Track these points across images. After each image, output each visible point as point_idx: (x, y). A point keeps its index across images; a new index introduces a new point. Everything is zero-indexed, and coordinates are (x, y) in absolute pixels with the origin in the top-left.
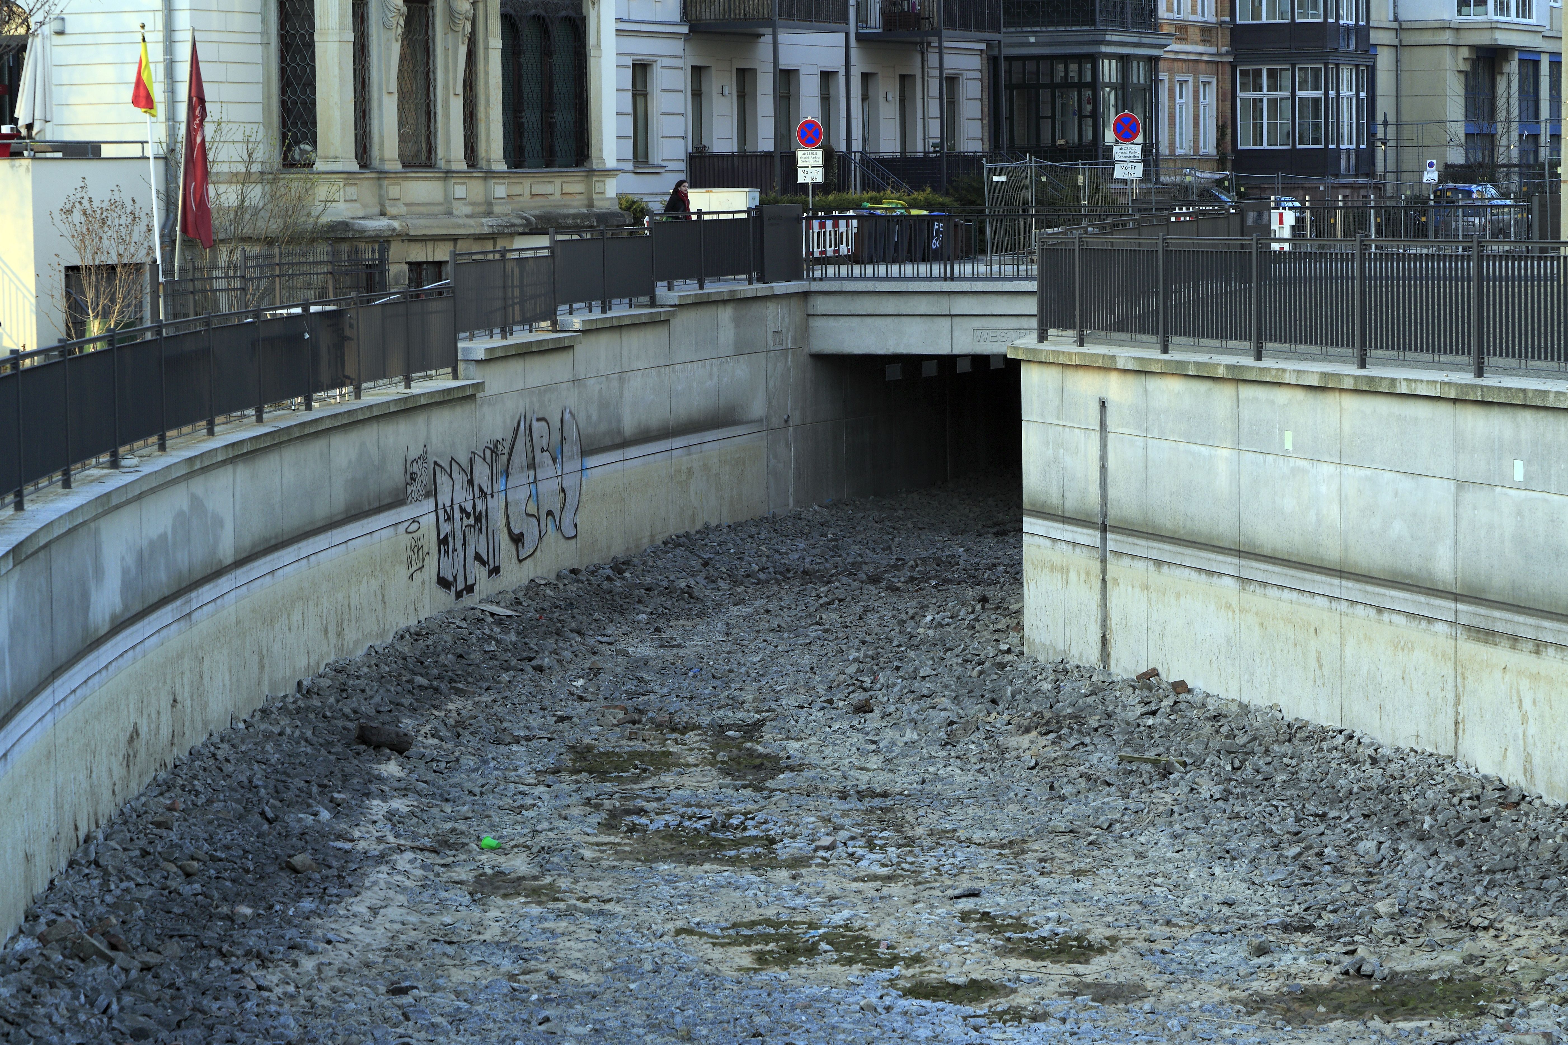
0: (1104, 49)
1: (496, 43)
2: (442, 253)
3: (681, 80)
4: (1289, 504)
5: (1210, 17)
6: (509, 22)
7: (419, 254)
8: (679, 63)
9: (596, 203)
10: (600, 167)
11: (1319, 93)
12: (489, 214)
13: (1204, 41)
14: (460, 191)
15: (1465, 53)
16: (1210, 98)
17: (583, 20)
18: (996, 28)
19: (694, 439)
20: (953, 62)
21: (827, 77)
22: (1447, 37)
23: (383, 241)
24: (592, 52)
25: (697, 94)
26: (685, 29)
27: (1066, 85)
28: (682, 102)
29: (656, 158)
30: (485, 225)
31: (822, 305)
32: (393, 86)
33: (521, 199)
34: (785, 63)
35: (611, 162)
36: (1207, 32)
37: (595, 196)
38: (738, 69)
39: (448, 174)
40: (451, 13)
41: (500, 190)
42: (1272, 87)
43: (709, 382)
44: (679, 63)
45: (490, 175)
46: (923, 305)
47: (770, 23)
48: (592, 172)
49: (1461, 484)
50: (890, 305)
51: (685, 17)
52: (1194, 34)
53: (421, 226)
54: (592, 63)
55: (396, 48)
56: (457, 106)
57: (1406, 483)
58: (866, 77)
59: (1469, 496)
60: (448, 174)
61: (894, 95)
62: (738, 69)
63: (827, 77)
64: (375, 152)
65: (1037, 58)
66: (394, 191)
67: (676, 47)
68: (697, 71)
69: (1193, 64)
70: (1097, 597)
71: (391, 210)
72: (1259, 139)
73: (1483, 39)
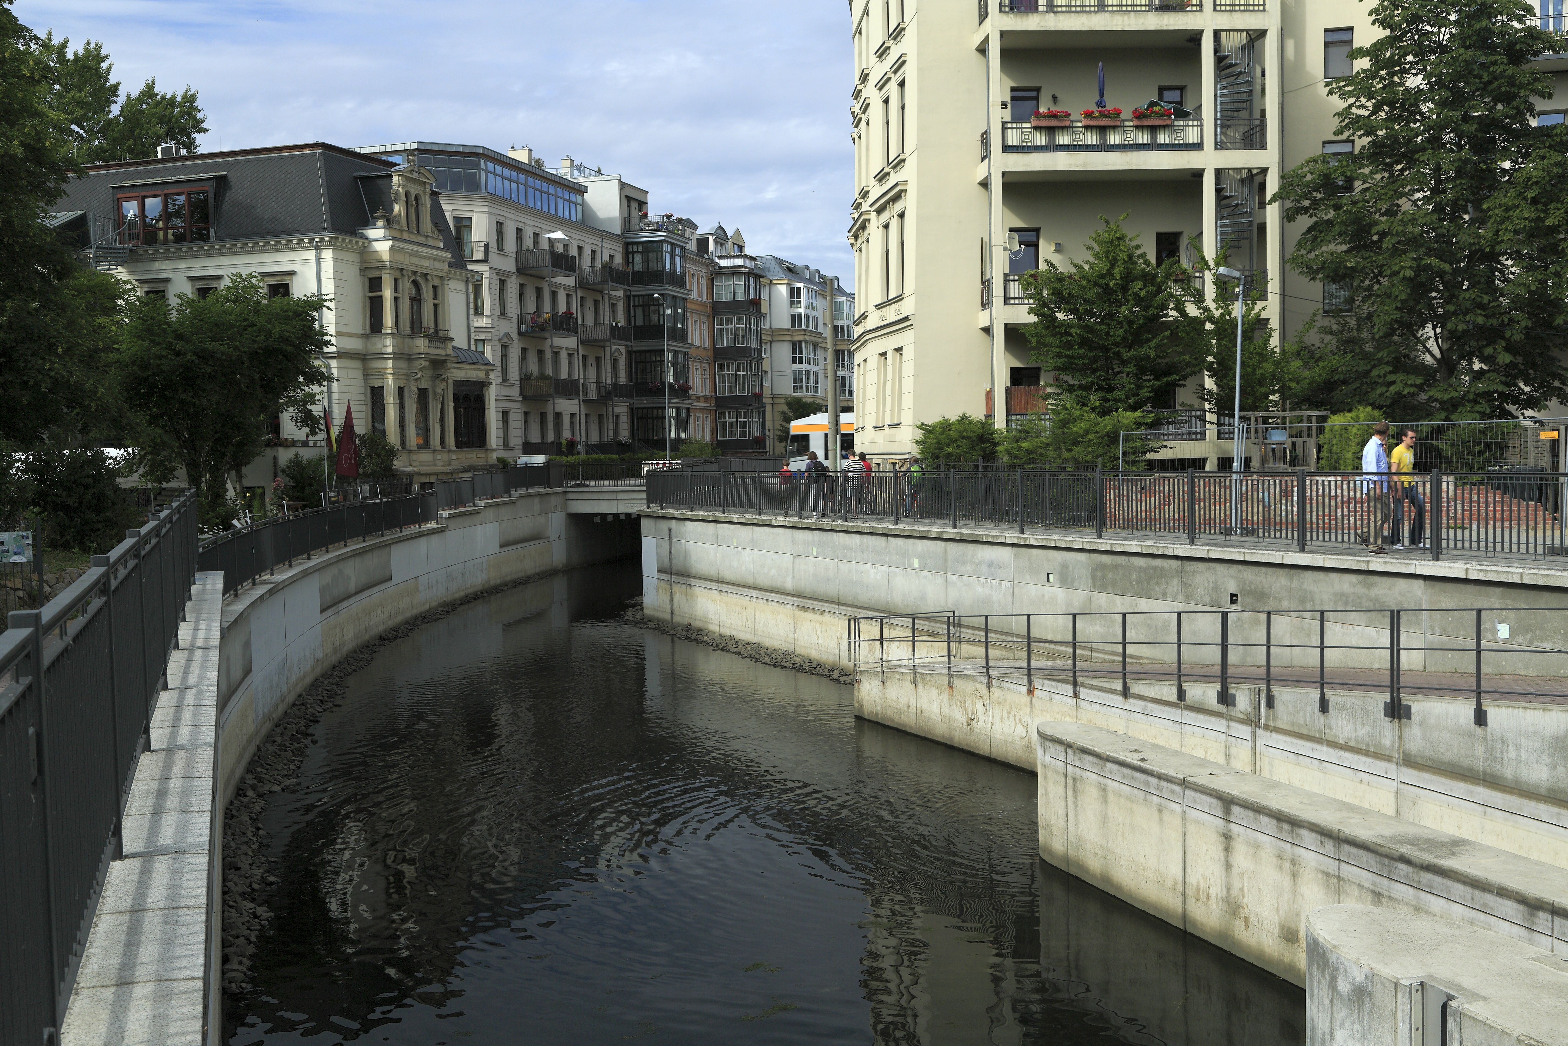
1: (451, 404)
2: (432, 479)
4: (735, 564)
5: (708, 394)
6: (456, 397)
7: (424, 480)
12: (450, 465)
14: (439, 457)
16: (708, 422)
17: (484, 395)
18: (632, 397)
19: (525, 544)
20: (617, 410)
21: (573, 415)
23: (411, 475)
24: (487, 407)
25: (526, 422)
29: (511, 444)
30: (448, 469)
31: (571, 496)
32: (414, 419)
34: (557, 410)
35: (494, 446)
36: (706, 399)
39: (435, 451)
40: (435, 394)
41: (454, 457)
45: (450, 451)
46: (607, 496)
47: (551, 396)
49: (795, 556)
50: (595, 496)
51: (521, 394)
52: (702, 399)
53: (425, 469)
54: (487, 411)
55: (415, 406)
56: (437, 427)
57: (775, 556)
58: (586, 415)
59: (798, 560)
60: (435, 451)
61: (597, 421)
63: (573, 415)
64: (407, 443)
66: (414, 457)
67: (518, 405)
69: (703, 410)
70: (669, 598)
71: (414, 464)
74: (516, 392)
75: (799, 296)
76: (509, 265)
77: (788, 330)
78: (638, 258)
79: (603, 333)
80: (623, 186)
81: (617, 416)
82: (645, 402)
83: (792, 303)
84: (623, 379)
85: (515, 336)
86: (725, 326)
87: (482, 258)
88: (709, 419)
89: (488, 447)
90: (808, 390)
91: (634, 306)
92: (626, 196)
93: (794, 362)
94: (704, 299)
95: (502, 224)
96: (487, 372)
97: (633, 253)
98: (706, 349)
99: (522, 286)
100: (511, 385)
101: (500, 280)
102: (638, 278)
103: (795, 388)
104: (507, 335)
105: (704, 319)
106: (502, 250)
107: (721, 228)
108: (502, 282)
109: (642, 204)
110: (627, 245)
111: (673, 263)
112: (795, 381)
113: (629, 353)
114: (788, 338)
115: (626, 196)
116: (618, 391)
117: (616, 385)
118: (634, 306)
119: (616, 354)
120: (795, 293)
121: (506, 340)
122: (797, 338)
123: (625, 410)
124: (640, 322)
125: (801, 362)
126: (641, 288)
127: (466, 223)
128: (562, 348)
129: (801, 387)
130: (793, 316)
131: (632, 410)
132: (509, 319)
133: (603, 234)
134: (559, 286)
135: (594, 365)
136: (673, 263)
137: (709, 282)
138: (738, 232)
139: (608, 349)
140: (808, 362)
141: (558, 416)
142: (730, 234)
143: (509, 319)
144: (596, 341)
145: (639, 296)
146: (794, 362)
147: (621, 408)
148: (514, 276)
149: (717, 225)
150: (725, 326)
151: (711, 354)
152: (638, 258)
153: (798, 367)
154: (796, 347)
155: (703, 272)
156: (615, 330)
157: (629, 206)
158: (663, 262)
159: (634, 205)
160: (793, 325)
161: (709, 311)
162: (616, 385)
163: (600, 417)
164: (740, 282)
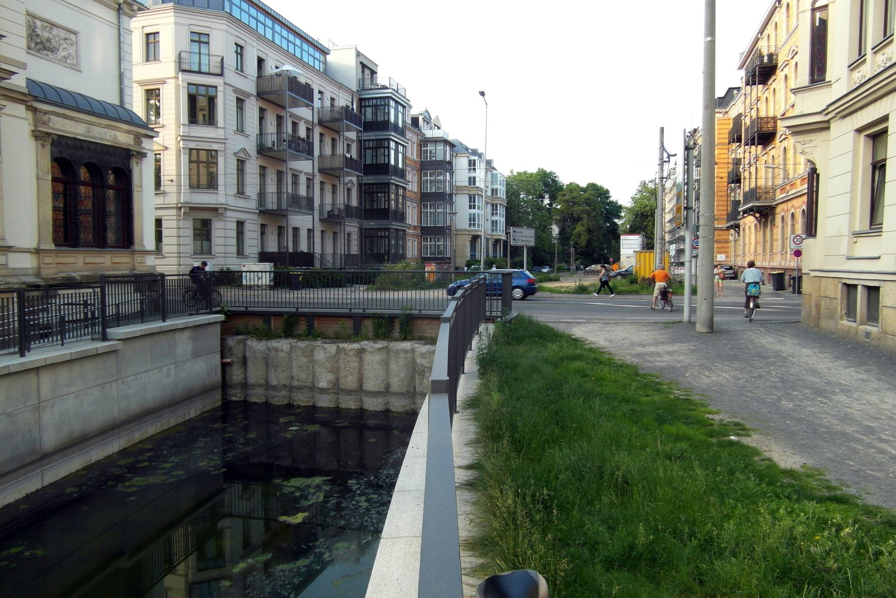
0: (392, 227)
3: (258, 228)
5: (415, 223)
8: (256, 222)
9: (137, 268)
10: (141, 249)
11: (437, 243)
13: (414, 230)
15: (471, 236)
17: (130, 171)
20: (348, 229)
21: (309, 230)
22: (467, 232)
25: (263, 233)
26: (258, 211)
27: (381, 237)
28: (257, 235)
29: (246, 252)
33: (75, 265)
36: (415, 228)
37: (136, 264)
38: (278, 226)
42: (430, 242)
43: (167, 380)
44: (256, 222)
48: (134, 252)
58: (322, 232)
61: (331, 237)
62: (278, 226)
63: (309, 230)
65: (373, 229)
67: (255, 217)
68: (263, 226)
69: (412, 235)
72: (427, 255)
73: (475, 233)
74: (253, 205)
75: (474, 165)
76: (249, 86)
77: (467, 187)
78: (369, 111)
79: (338, 163)
80: (358, 54)
81: (349, 234)
82: (372, 224)
83: (470, 170)
84: (354, 203)
85: (252, 150)
86: (429, 178)
87: (219, 71)
88: (416, 242)
89: (137, 247)
90: (478, 227)
91: (365, 149)
92: (361, 63)
93: (470, 208)
94: (415, 158)
95: (242, 48)
96: (138, 138)
97: (365, 107)
98: (415, 193)
99: (262, 110)
100: (248, 198)
101: (238, 99)
102: (369, 126)
103: (470, 225)
104: (244, 150)
105: (415, 172)
106: (242, 71)
107: (427, 111)
108: (240, 102)
109: (373, 73)
110: (361, 100)
111: (396, 117)
112: (470, 220)
113: (360, 185)
114: (468, 192)
115: (361, 63)
116: (349, 211)
117: (348, 207)
118: (365, 149)
119: (349, 185)
120: (472, 164)
121: (242, 155)
122: (472, 193)
123: (356, 230)
124: (369, 162)
125: (474, 208)
126: (371, 134)
127: (204, 39)
128: (301, 172)
129: (474, 225)
130: (470, 178)
131: (361, 230)
132: (247, 136)
133: (341, 86)
134: (301, 119)
135: (330, 190)
136: (396, 117)
137: (419, 147)
138: (437, 117)
139: (342, 178)
140: (479, 209)
141: (296, 230)
142: (433, 118)
143: (247, 136)
144: (331, 169)
145: (369, 140)
146: (470, 208)
147: (352, 228)
148: (253, 99)
149: (425, 109)
150: (429, 178)
151: (419, 196)
152: (369, 111)
153: (472, 211)
154: (472, 199)
155: (415, 139)
156: (349, 162)
157: (363, 72)
158: (389, 113)
159: (367, 72)
160: (470, 184)
161: (418, 167)
162: (348, 207)
163: (335, 234)
164: (440, 147)
